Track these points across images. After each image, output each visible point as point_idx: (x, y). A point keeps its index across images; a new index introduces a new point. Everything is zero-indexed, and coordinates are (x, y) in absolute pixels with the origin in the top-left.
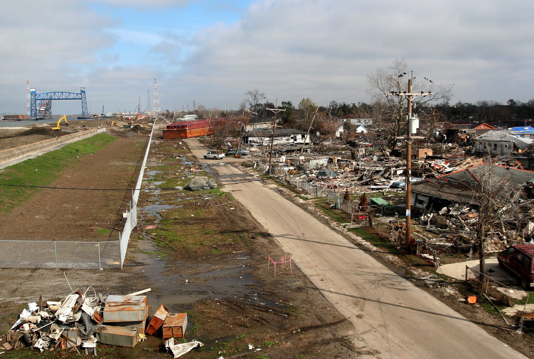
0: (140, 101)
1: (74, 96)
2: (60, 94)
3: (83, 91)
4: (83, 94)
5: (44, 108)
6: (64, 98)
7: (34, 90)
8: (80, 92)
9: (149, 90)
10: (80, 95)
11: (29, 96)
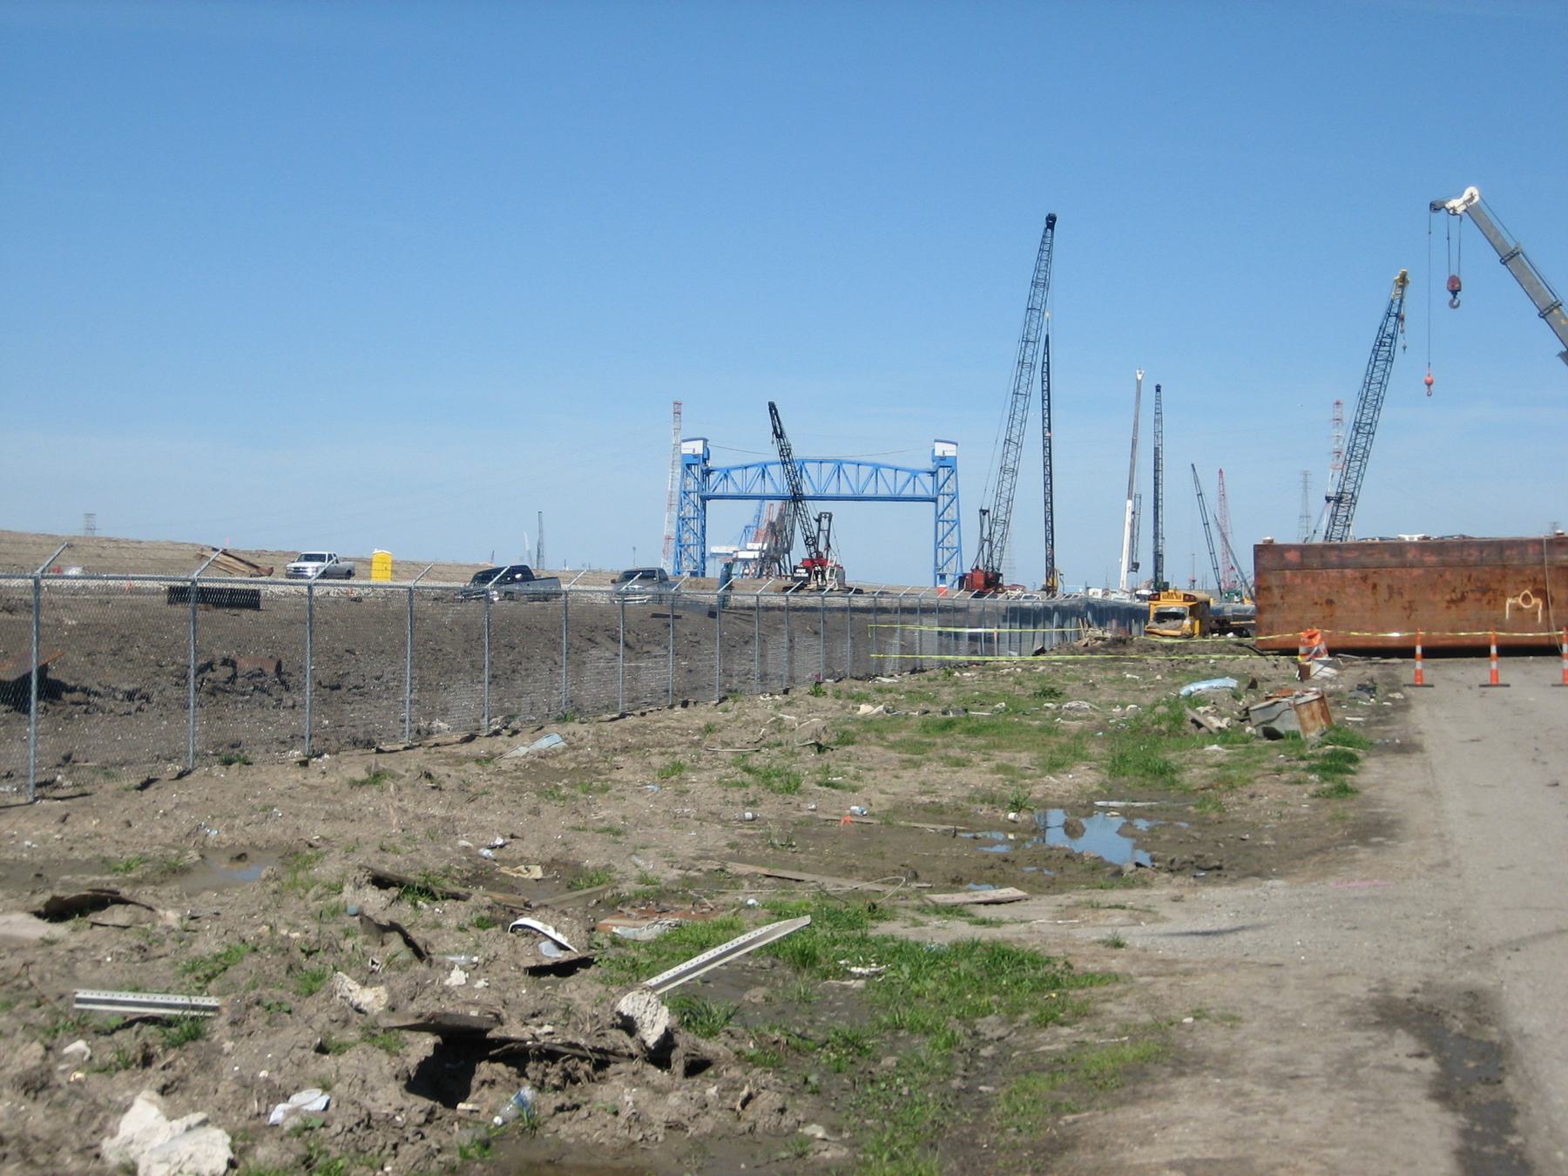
0: (1197, 481)
1: (900, 483)
2: (828, 468)
3: (943, 458)
4: (943, 473)
5: (757, 546)
6: (846, 491)
7: (698, 447)
8: (930, 466)
9: (1306, 474)
10: (928, 480)
11: (671, 479)
